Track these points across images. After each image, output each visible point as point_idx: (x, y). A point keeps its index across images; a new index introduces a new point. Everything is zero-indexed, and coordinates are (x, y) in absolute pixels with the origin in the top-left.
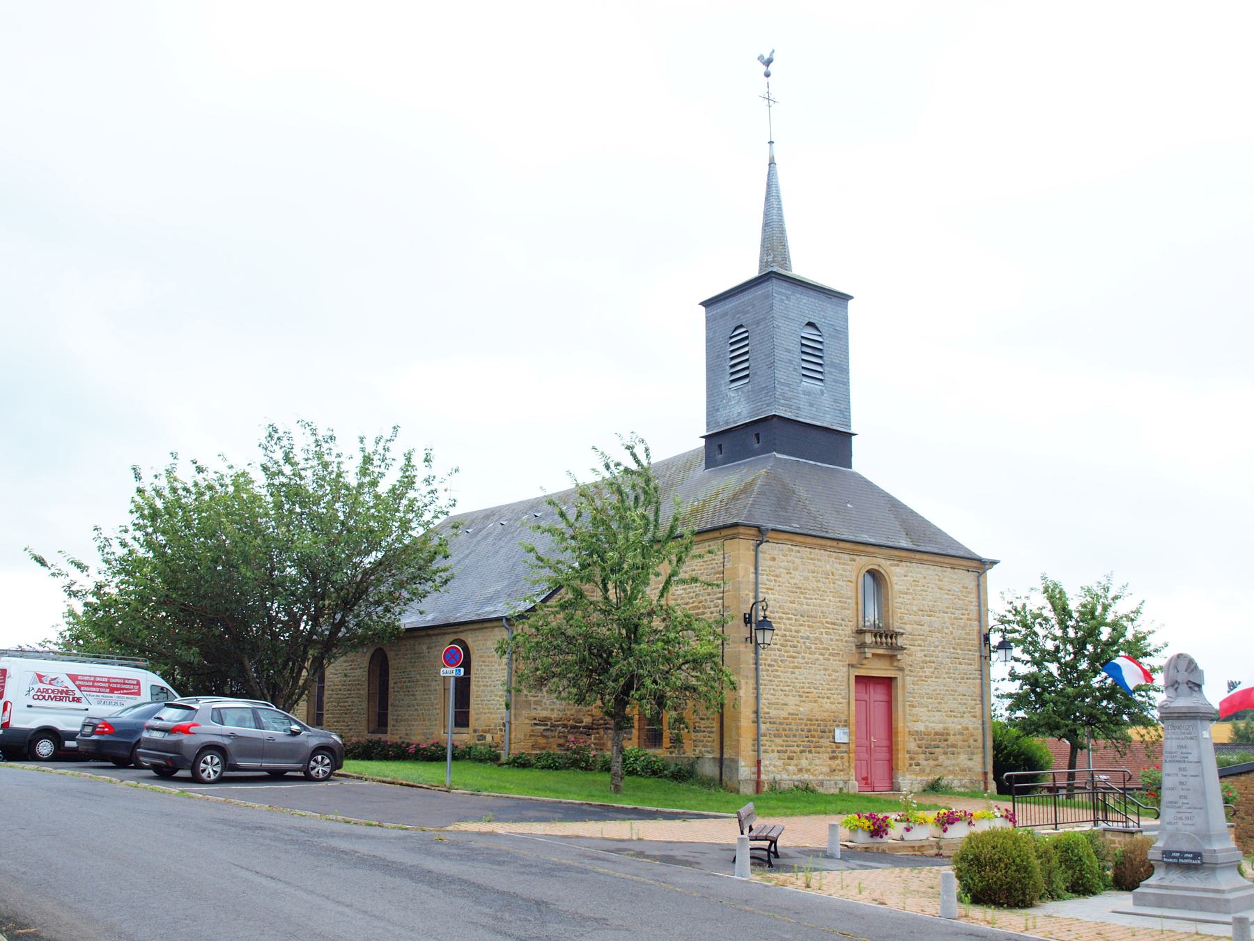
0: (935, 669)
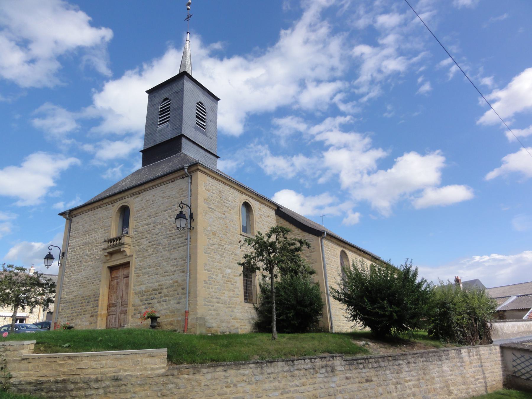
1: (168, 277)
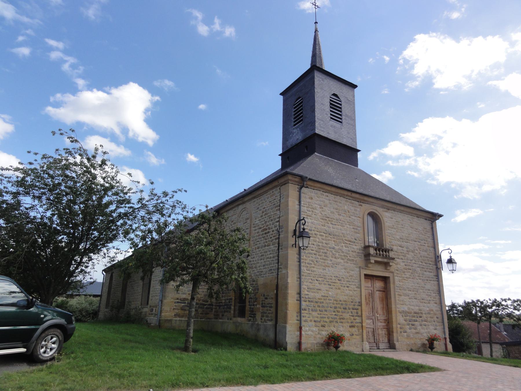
1: (425, 304)
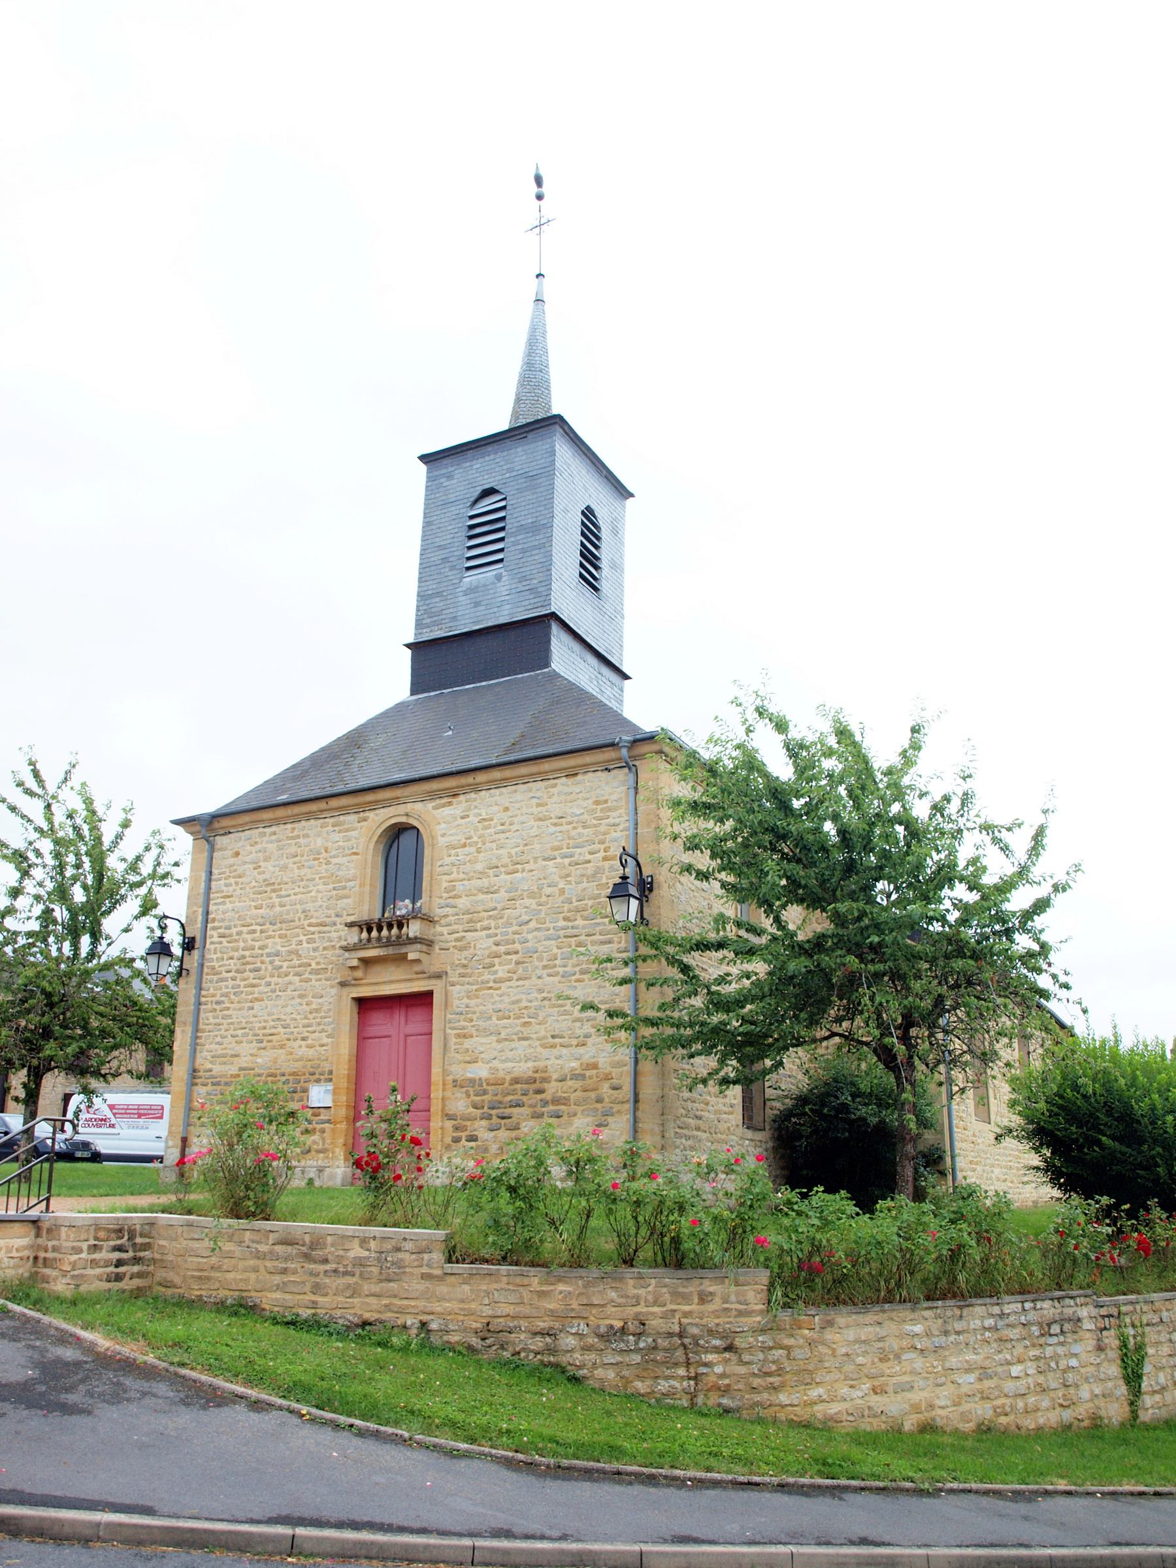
0: (518, 963)
1: (564, 1051)
